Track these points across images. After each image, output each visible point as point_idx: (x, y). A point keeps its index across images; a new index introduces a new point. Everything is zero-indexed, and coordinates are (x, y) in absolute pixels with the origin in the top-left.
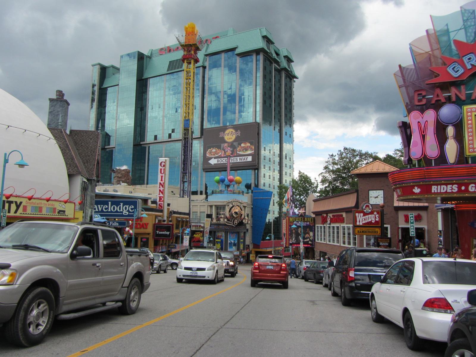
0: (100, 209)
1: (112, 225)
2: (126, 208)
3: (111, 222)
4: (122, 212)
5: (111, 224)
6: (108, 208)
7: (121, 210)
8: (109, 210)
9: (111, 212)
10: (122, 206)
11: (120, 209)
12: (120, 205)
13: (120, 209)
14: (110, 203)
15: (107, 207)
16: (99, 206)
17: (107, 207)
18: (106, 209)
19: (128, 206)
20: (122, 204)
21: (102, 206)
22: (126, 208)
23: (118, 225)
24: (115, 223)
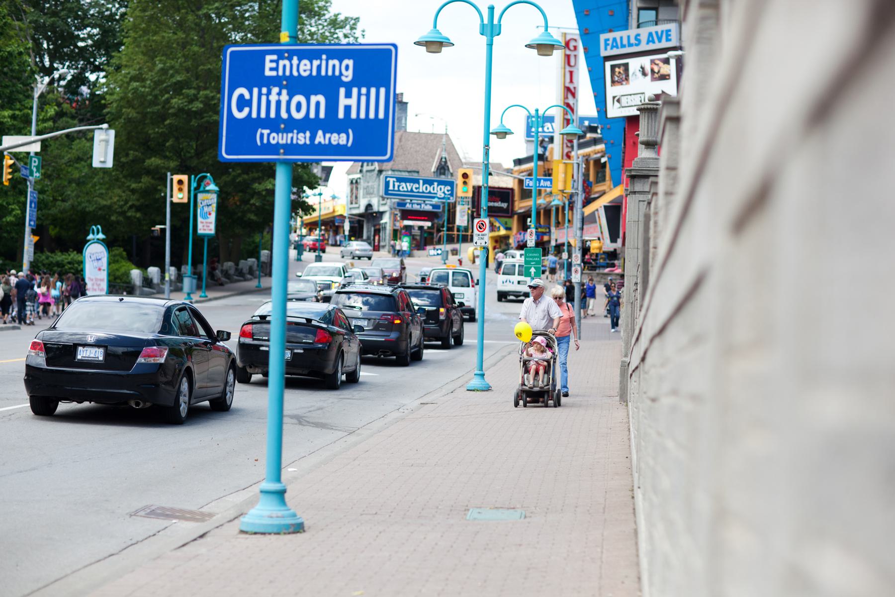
0: (409, 189)
2: (441, 189)
6: (419, 188)
7: (435, 191)
9: (423, 192)
11: (434, 189)
13: (434, 189)
14: (421, 182)
15: (417, 186)
16: (408, 184)
17: (417, 186)
18: (416, 188)
21: (412, 184)
22: (441, 189)
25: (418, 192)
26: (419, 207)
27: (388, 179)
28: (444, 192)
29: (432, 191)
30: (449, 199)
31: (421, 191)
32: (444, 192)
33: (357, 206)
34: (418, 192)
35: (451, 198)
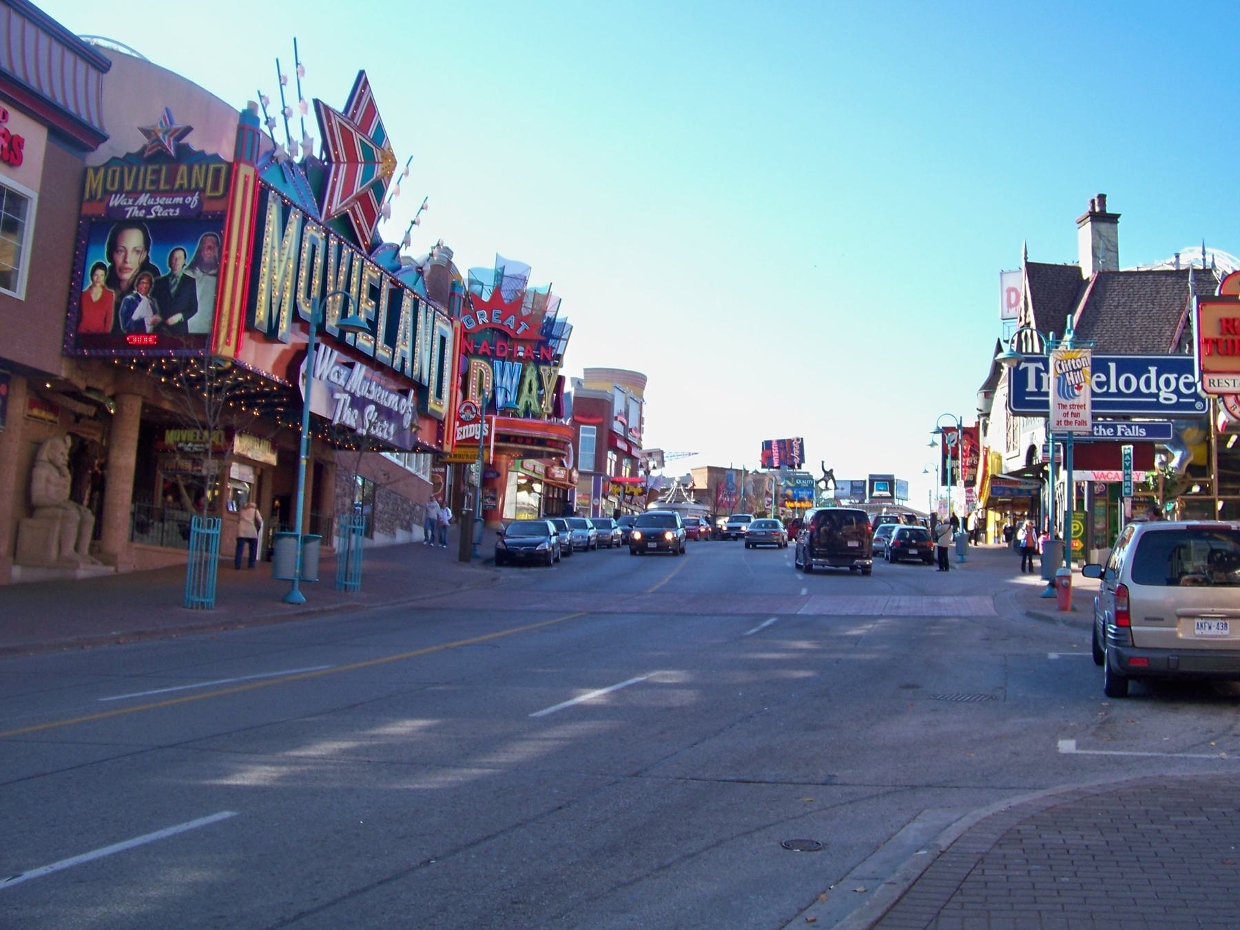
1: (1126, 434)
3: (1119, 427)
4: (1157, 396)
5: (1122, 433)
6: (1108, 383)
7: (1153, 390)
8: (1113, 389)
9: (1119, 393)
10: (1153, 375)
11: (1148, 385)
12: (1149, 372)
13: (1148, 385)
14: (1113, 366)
15: (1103, 378)
17: (1103, 378)
19: (1176, 376)
20: (1153, 370)
23: (1145, 434)
24: (1133, 427)
25: (1107, 394)
26: (1110, 431)
27: (1023, 365)
28: (1177, 391)
29: (1143, 389)
30: (1191, 406)
31: (1113, 389)
32: (1177, 391)
33: (1016, 453)
34: (1107, 394)
35: (1199, 405)
